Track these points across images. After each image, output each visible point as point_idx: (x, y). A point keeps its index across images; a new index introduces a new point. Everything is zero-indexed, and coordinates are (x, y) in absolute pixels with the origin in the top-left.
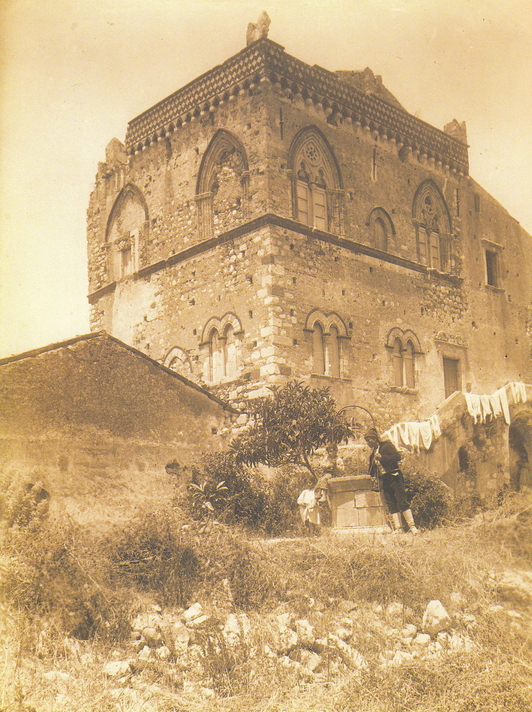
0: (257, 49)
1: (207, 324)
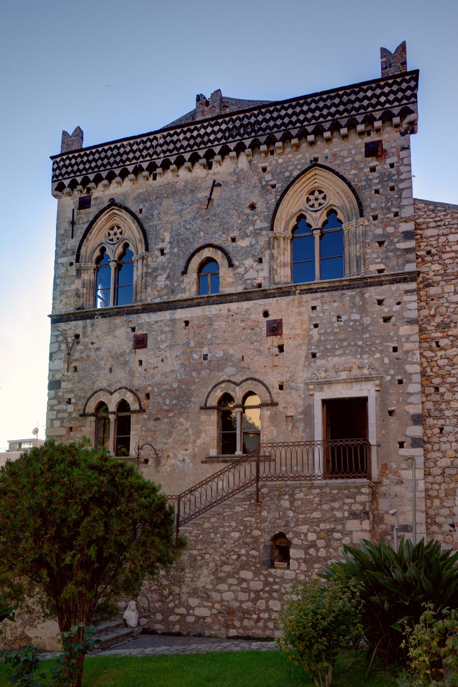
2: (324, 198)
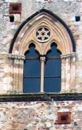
2: (49, 34)
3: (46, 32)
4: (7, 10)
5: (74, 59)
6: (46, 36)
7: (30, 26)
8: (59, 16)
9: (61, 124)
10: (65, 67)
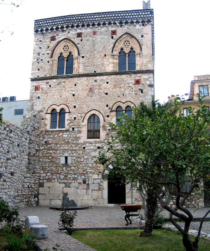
0: (149, 12)
1: (115, 103)
2: (129, 44)
3: (128, 43)
4: (110, 33)
5: (141, 55)
6: (128, 44)
7: (121, 40)
8: (134, 35)
9: (136, 84)
10: (137, 59)
